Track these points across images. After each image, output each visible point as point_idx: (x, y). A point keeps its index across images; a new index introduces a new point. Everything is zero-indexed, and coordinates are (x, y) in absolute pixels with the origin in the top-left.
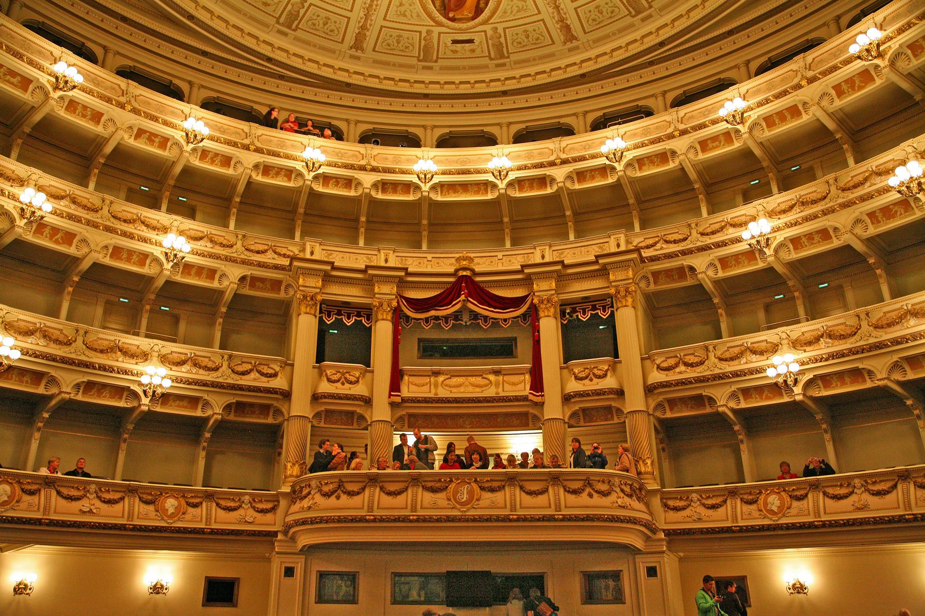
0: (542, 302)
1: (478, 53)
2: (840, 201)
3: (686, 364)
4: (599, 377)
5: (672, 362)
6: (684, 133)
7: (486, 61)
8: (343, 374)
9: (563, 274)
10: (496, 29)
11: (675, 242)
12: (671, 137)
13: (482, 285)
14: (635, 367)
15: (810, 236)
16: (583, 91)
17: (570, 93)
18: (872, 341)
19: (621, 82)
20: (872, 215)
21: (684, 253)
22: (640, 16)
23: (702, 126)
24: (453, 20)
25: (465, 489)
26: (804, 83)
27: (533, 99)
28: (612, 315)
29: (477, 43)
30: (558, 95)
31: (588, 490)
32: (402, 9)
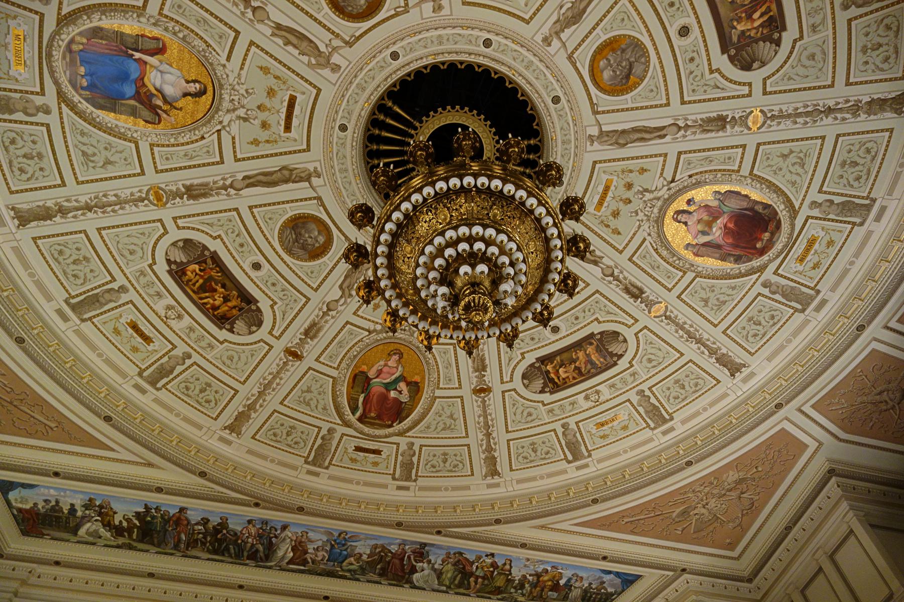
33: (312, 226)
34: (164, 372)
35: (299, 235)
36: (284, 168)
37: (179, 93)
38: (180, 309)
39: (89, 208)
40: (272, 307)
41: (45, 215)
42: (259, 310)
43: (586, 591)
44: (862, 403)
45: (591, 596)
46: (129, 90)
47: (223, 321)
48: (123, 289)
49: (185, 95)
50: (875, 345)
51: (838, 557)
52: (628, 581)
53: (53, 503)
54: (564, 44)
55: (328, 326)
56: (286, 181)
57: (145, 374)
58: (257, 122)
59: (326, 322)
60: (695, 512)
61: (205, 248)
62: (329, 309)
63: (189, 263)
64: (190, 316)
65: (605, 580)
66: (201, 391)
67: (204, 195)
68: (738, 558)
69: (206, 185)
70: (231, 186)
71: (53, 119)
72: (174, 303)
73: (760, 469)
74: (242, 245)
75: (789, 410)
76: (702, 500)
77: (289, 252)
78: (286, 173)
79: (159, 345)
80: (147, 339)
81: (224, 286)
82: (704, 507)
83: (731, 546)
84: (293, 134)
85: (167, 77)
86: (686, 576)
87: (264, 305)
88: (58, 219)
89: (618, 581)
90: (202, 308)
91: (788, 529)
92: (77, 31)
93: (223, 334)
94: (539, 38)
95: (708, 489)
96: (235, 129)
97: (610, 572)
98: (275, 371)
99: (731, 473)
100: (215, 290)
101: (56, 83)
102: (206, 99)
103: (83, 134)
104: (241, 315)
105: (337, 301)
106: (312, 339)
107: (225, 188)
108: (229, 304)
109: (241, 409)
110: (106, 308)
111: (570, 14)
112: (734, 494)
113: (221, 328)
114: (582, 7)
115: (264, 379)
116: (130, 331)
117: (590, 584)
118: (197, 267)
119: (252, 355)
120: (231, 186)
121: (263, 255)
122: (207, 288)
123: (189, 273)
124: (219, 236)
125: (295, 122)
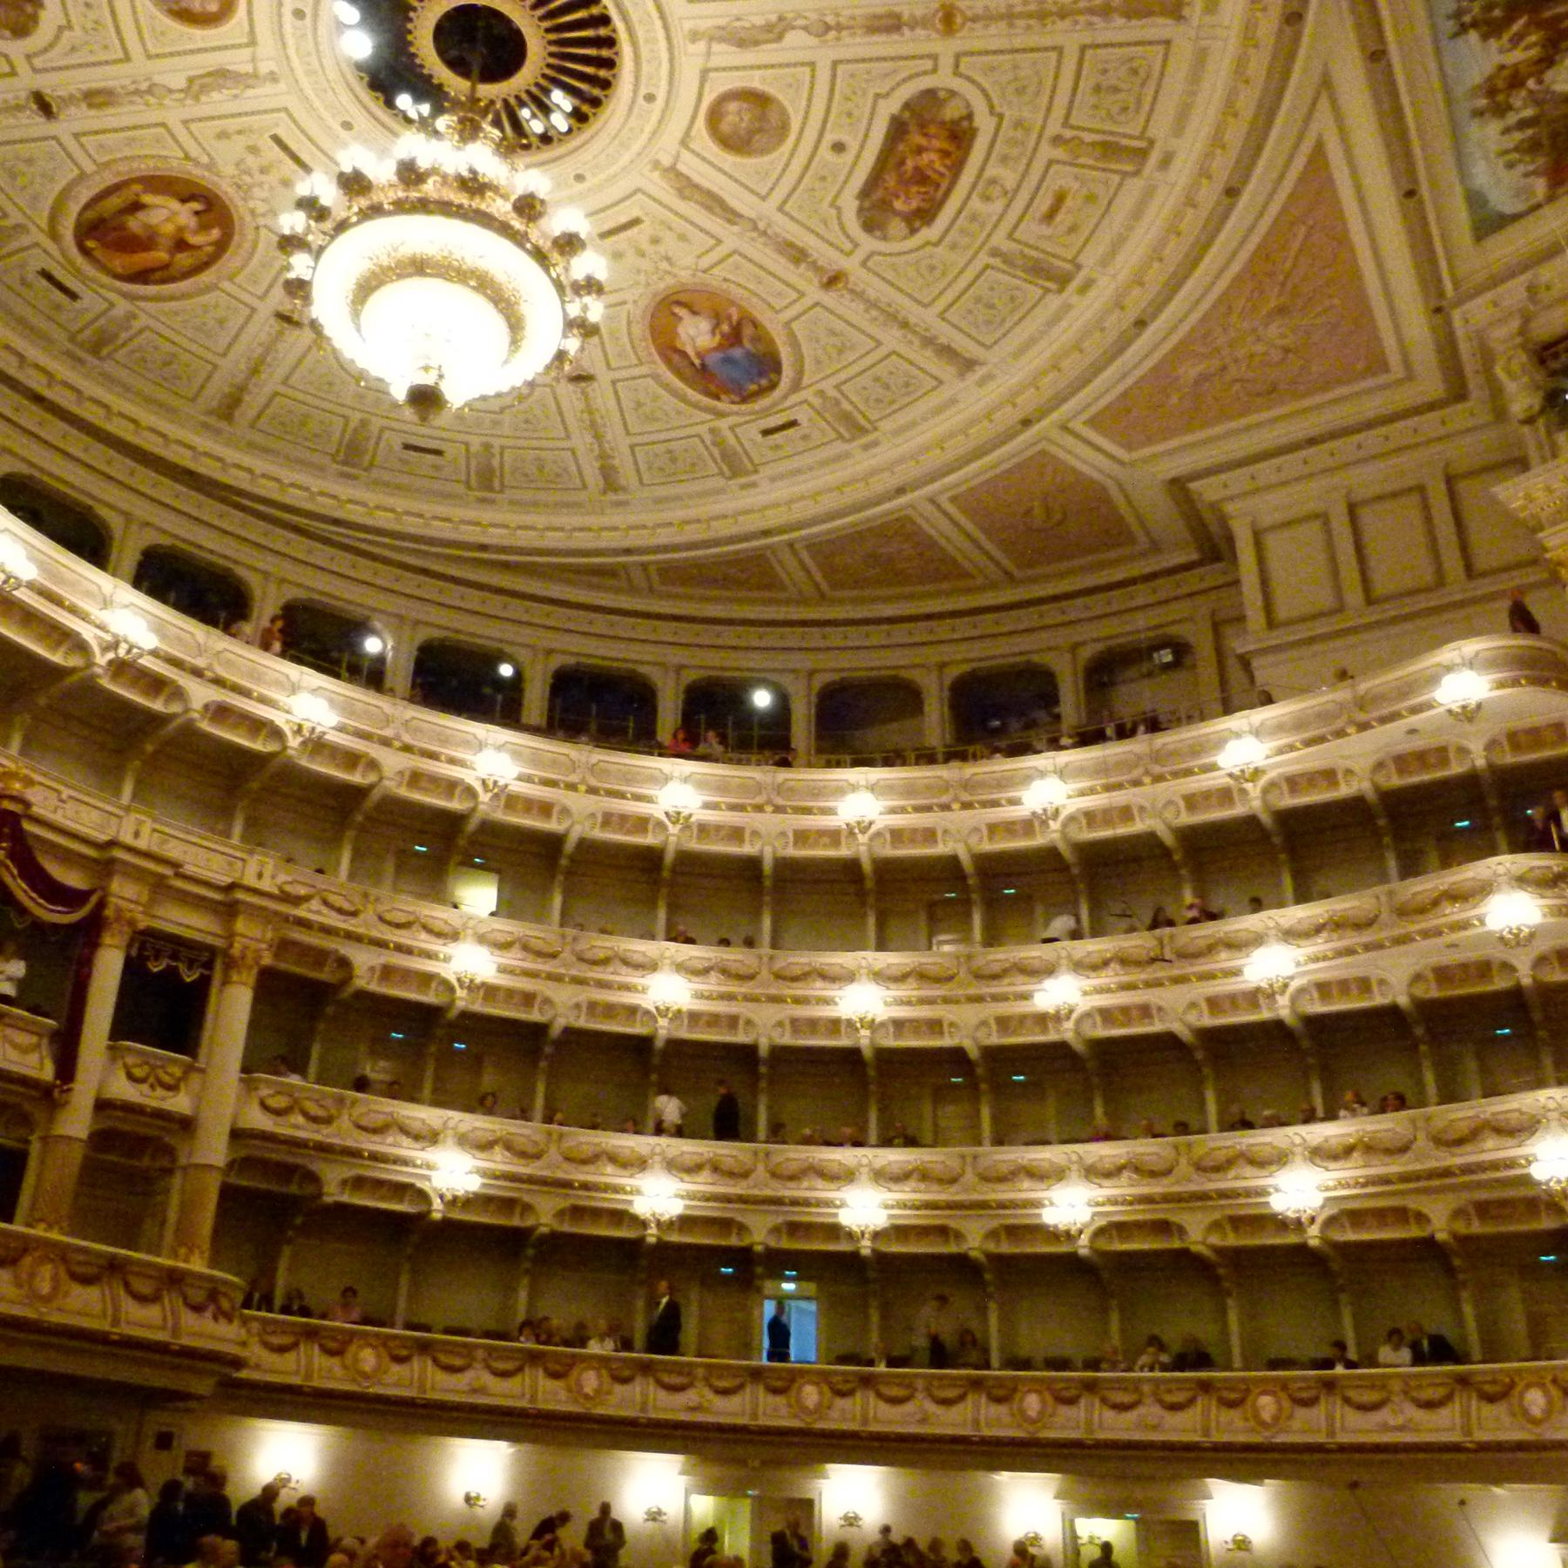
0: (118, 918)
1: (62, 317)
2: (574, 972)
3: (306, 1115)
4: (169, 1088)
5: (279, 1102)
6: (407, 748)
7: (60, 336)
8: (153, 1068)
9: (165, 883)
10: (134, 317)
11: (340, 911)
12: (386, 742)
13: (31, 842)
14: (222, 1095)
15: (510, 993)
16: (167, 490)
17: (144, 478)
18: (560, 1175)
19: (234, 520)
20: (592, 1006)
21: (350, 936)
22: (346, 469)
23: (433, 756)
24: (85, 252)
25: (47, 1271)
26: (583, 788)
27: (77, 443)
28: (204, 984)
29: (77, 305)
30: (120, 466)
31: (212, 1308)
32: (22, 167)
33: (725, 127)
34: (1110, 150)
35: (751, 133)
36: (683, 197)
37: (697, 319)
38: (980, 187)
39: (905, 325)
40: (887, 95)
41: (947, 352)
42: (907, 106)
46: (737, 353)
47: (960, 136)
48: (995, 253)
49: (695, 313)
53: (1516, 156)
54: (253, 60)
55: (857, 12)
56: (697, 187)
57: (1128, 168)
58: (662, 249)
59: (853, 18)
61: (860, 210)
62: (828, 28)
63: (896, 213)
64: (982, 169)
66: (1116, 90)
67: (792, 245)
69: (780, 252)
70: (755, 228)
71: (824, 385)
72: (974, 196)
74: (823, 178)
77: (784, 127)
78: (687, 192)
79: (1062, 178)
80: (1060, 199)
81: (902, 163)
84: (636, 212)
85: (692, 332)
87: (892, 106)
88: (943, 340)
90: (957, 168)
92: (720, 405)
93: (984, 123)
94: (282, 86)
96: (689, 260)
98: (1003, 25)
100: (917, 169)
101: (785, 397)
102: (683, 297)
103: (818, 362)
104: (932, 121)
105: (805, 28)
106: (898, 16)
107: (764, 233)
108: (923, 141)
109: (1120, 21)
110: (1034, 253)
111: (229, 83)
113: (972, 133)
114: (207, 80)
115: (1029, 27)
116: (1059, 217)
118: (898, 205)
119: (993, 69)
120: (755, 228)
121: (816, 148)
122: (921, 177)
123: (914, 205)
124: (833, 205)
125: (623, 220)
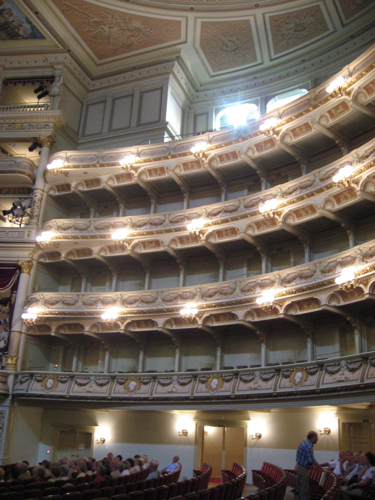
43: (7, 23)
44: (220, 39)
45: (7, 28)
50: (252, 19)
51: (145, 95)
52: (35, 35)
60: (103, 27)
65: (24, 25)
68: (98, 65)
73: (152, 31)
75: (191, 15)
76: (112, 24)
82: (109, 28)
83: (101, 57)
86: (67, 55)
89: (30, 31)
91: (134, 68)
95: (120, 21)
97: (29, 22)
99: (139, 22)
112: (129, 33)
117: (13, 21)
